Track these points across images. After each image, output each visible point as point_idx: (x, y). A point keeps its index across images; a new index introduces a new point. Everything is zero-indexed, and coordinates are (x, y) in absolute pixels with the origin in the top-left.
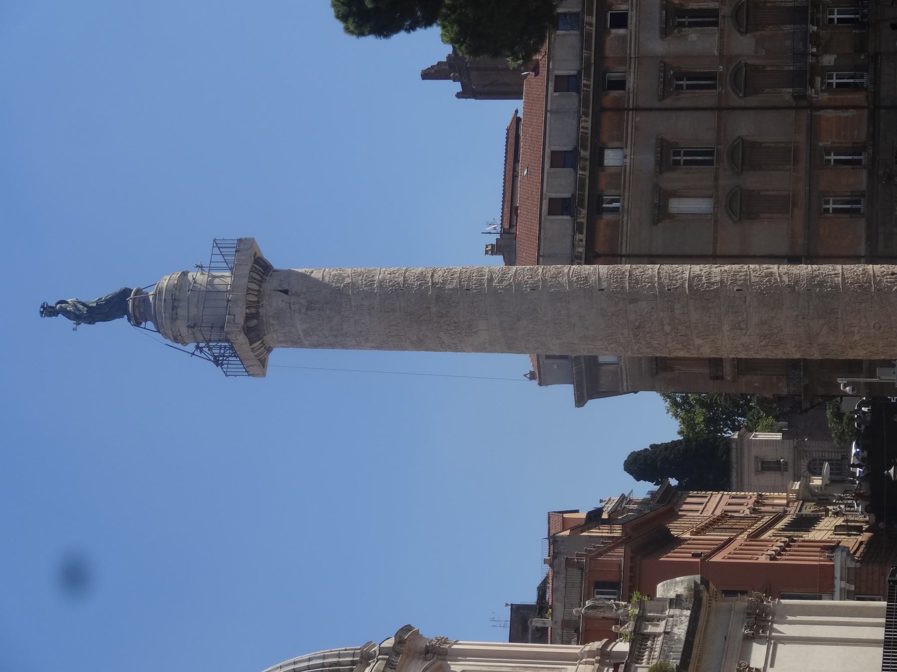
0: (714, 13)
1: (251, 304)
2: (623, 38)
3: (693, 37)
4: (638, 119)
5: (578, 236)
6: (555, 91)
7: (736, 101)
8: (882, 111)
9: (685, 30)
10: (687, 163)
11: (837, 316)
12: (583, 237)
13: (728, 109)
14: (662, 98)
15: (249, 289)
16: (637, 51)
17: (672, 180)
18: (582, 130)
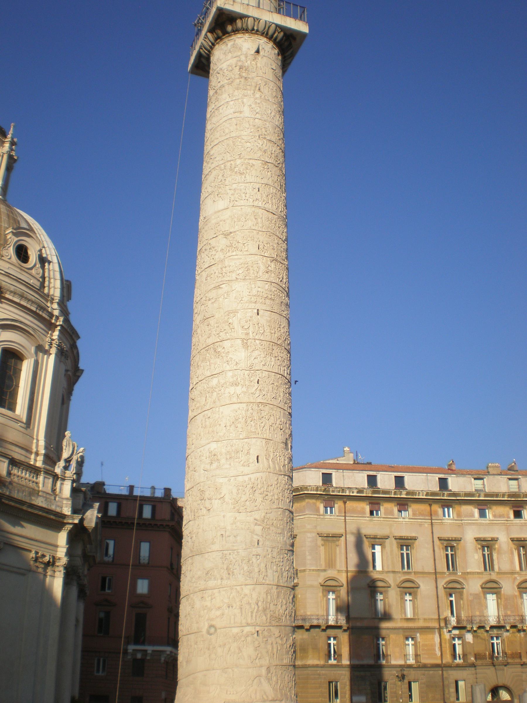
0: (492, 568)
1: (245, 22)
2: (473, 515)
3: (476, 557)
4: (426, 525)
5: (355, 491)
6: (439, 478)
7: (442, 583)
8: (441, 672)
9: (480, 552)
10: (402, 555)
11: (225, 578)
12: (355, 494)
13: (436, 578)
14: (440, 539)
15: (259, 20)
16: (466, 524)
17: (392, 545)
18: (417, 493)
